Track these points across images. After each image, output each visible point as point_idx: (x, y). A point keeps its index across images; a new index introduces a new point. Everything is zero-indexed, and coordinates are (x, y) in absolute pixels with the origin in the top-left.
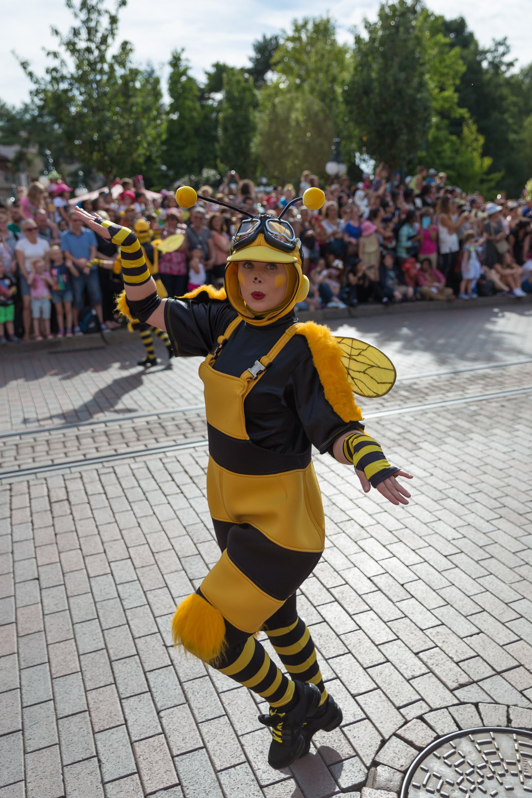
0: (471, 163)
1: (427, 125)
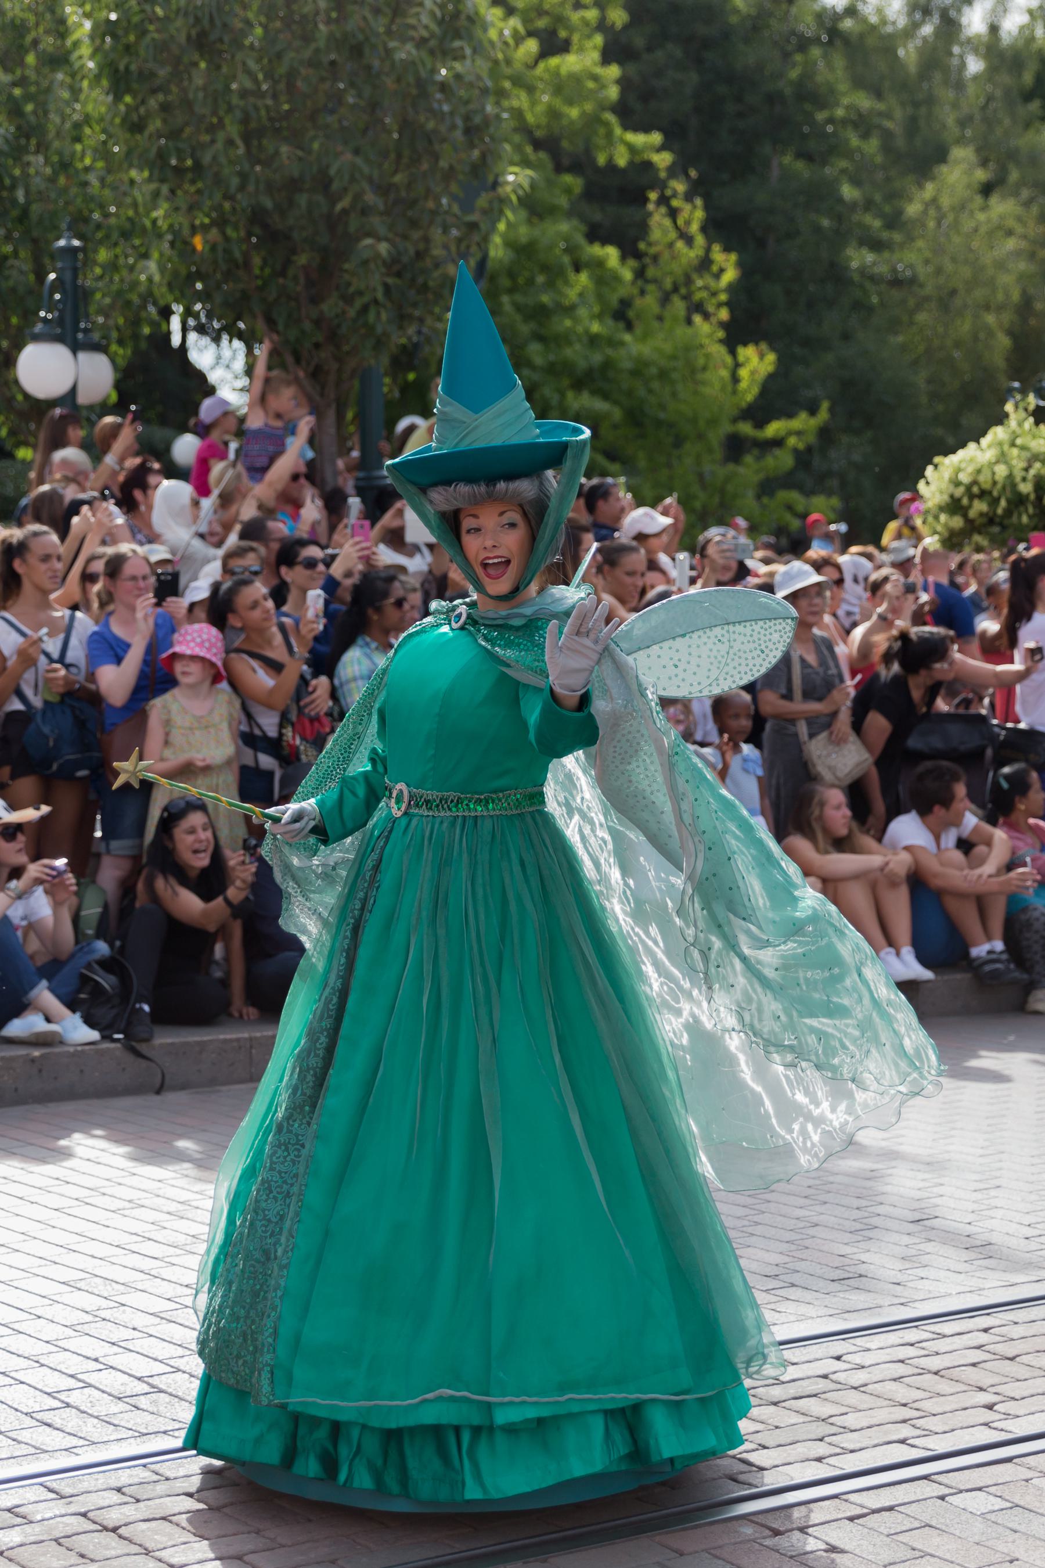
0: (687, 364)
1: (482, 201)
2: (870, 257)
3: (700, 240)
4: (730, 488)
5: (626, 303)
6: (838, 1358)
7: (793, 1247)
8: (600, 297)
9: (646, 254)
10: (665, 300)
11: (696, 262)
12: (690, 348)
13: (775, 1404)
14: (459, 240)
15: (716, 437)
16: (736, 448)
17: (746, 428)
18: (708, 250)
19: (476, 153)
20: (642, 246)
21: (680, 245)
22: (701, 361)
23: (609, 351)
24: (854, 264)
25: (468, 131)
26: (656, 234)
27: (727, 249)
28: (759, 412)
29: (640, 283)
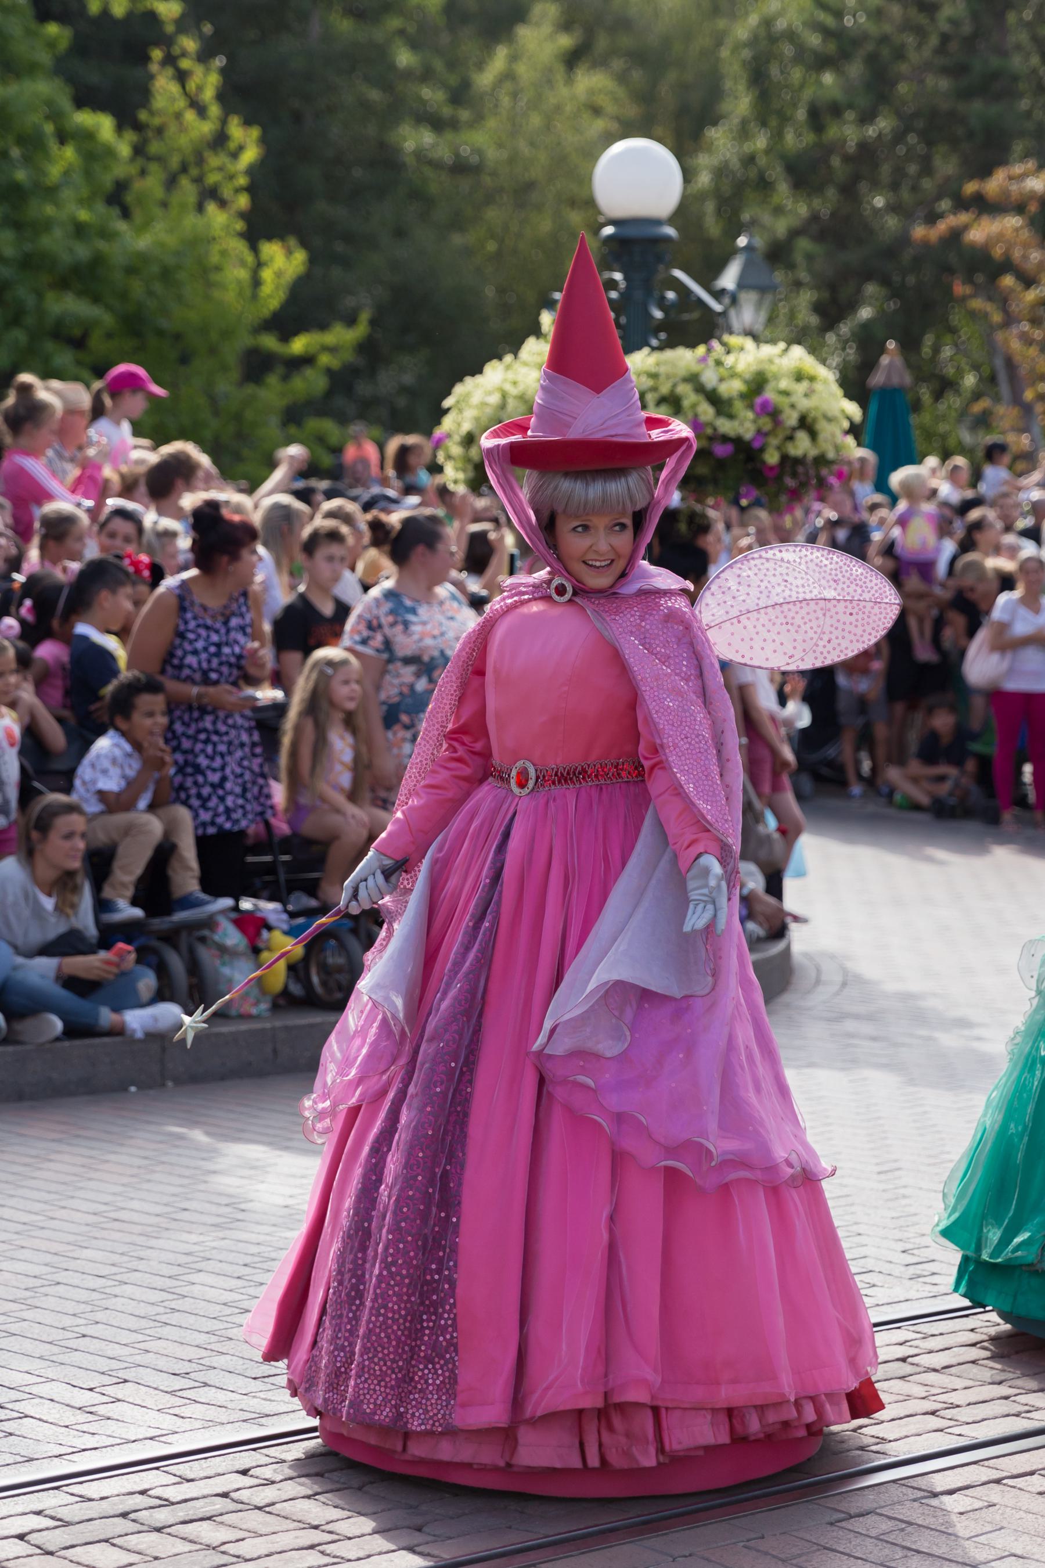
0: (193, 263)
2: (427, 137)
3: (214, 110)
4: (249, 415)
5: (121, 187)
6: (244, 1472)
7: (214, 1338)
8: (88, 174)
9: (147, 126)
10: (171, 182)
11: (209, 137)
12: (199, 242)
13: (159, 1530)
15: (232, 352)
16: (257, 366)
17: (269, 342)
18: (224, 122)
20: (143, 116)
21: (190, 116)
22: (215, 259)
23: (101, 245)
24: (409, 145)
26: (159, 102)
27: (247, 122)
28: (286, 322)
29: (140, 161)
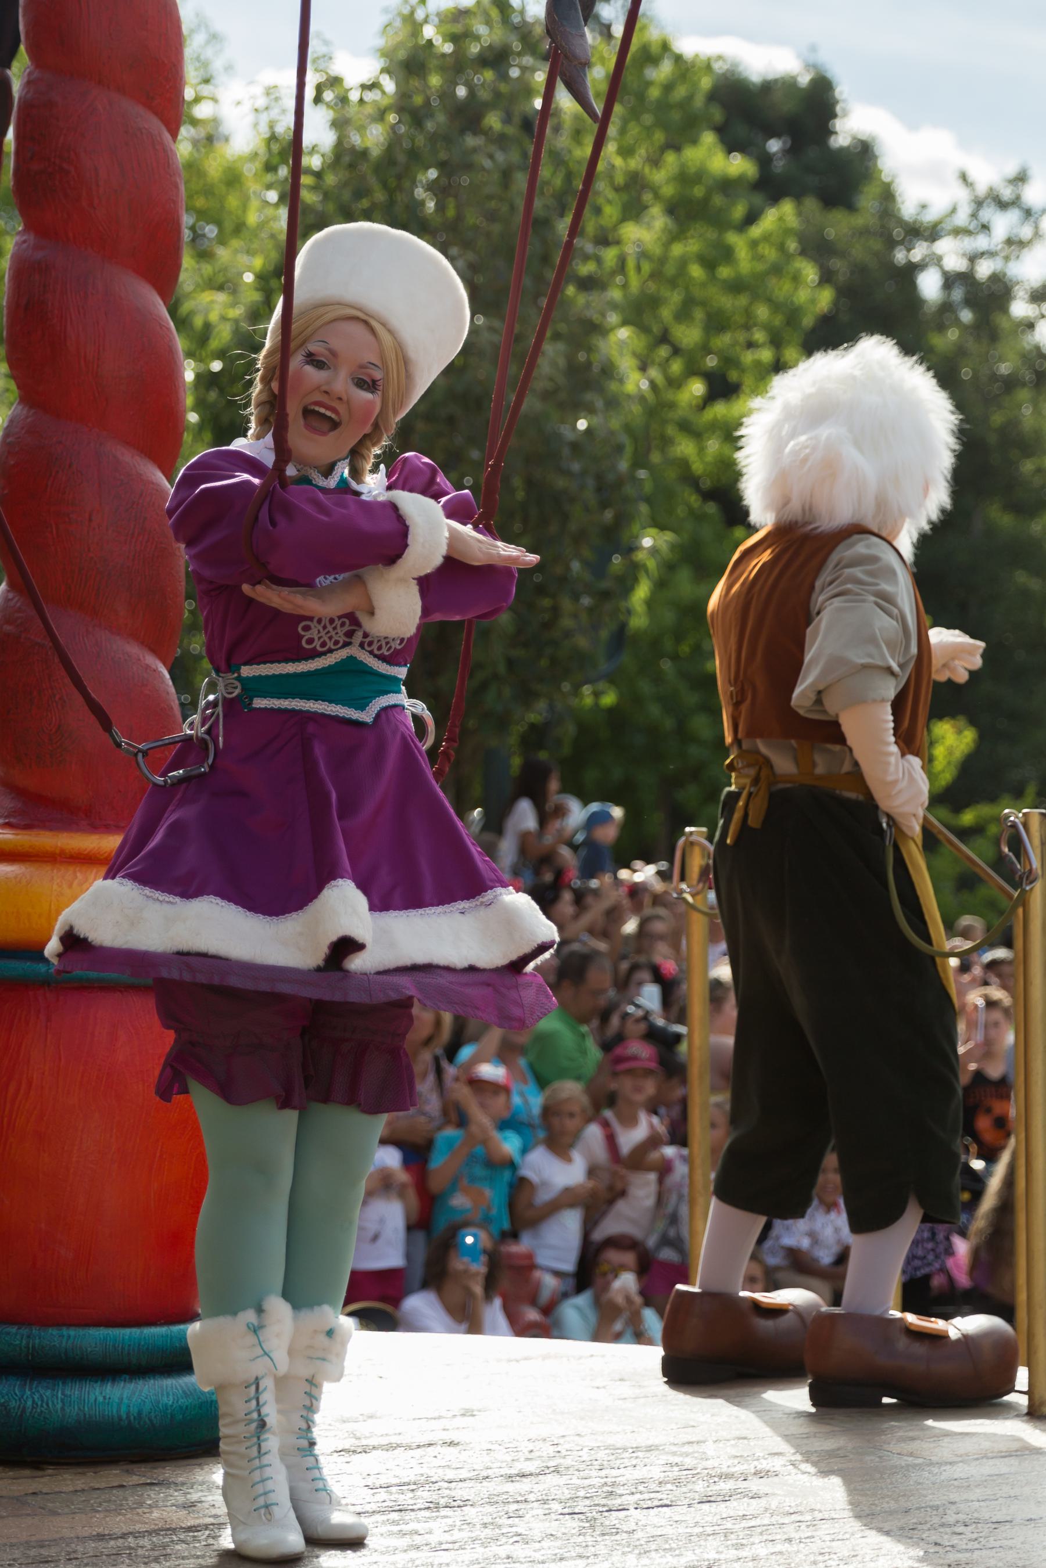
14: (591, 610)
19: (609, 515)
25: (599, 489)
